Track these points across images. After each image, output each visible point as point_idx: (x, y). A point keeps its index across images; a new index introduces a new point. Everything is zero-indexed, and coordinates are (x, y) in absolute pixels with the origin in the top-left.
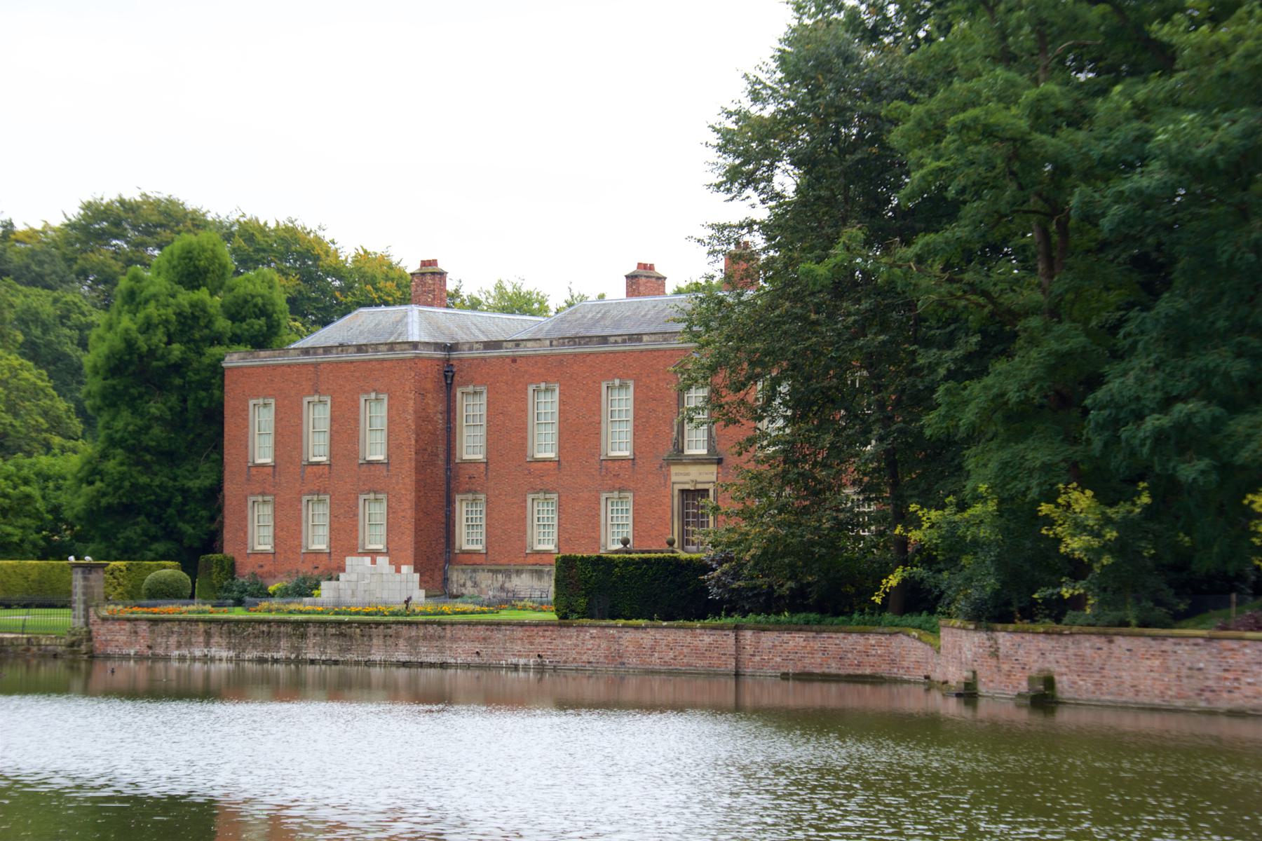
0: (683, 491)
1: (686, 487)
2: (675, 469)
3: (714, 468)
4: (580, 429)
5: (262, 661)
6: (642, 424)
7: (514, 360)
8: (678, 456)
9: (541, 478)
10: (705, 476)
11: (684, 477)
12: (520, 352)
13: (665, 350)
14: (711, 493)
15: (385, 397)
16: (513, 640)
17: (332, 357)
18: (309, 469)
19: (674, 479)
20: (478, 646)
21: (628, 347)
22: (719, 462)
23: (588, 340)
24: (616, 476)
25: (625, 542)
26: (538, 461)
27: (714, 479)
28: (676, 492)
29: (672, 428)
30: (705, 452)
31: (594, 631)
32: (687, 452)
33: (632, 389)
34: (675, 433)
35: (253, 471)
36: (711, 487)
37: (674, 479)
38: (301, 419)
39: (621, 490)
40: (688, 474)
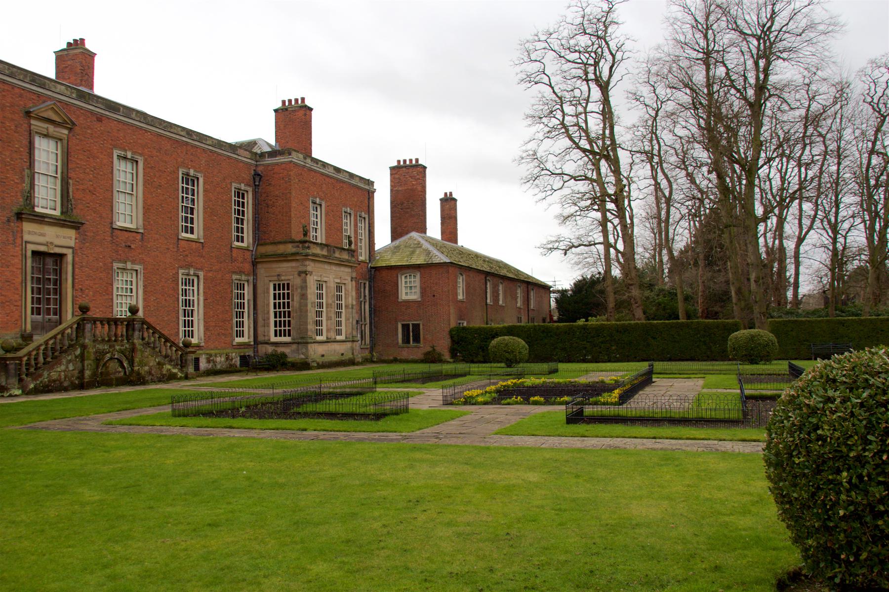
0: (34, 253)
1: (42, 249)
3: (72, 233)
8: (26, 213)
13: (13, 86)
14: (70, 258)
19: (26, 237)
22: (76, 225)
25: (133, 310)
27: (73, 245)
28: (29, 254)
29: (22, 178)
30: (57, 213)
32: (37, 210)
34: (26, 186)
36: (69, 252)
37: (26, 237)
40: (43, 235)
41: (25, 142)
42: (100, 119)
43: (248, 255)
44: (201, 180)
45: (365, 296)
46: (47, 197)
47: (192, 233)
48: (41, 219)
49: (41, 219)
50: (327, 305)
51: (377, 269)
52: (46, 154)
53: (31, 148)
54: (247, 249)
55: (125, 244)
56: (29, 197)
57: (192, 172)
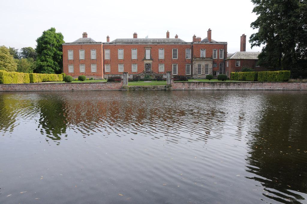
2: (145, 61)
3: (152, 61)
4: (128, 55)
5: (218, 90)
6: (139, 54)
7: (115, 45)
8: (145, 59)
9: (121, 62)
10: (151, 62)
11: (146, 62)
12: (116, 44)
15: (96, 50)
16: (278, 85)
17: (85, 44)
18: (81, 60)
20: (270, 86)
21: (136, 44)
23: (129, 43)
24: (134, 62)
26: (120, 60)
31: (295, 83)
33: (137, 50)
35: (69, 61)
38: (79, 53)
39: (135, 64)
41: (144, 51)
42: (156, 45)
43: (190, 61)
44: (177, 50)
45: (222, 66)
46: (148, 57)
47: (176, 58)
48: (146, 60)
49: (146, 60)
50: (203, 68)
51: (225, 60)
52: (148, 52)
53: (145, 51)
54: (190, 59)
55: (161, 62)
56: (145, 58)
57: (175, 49)
